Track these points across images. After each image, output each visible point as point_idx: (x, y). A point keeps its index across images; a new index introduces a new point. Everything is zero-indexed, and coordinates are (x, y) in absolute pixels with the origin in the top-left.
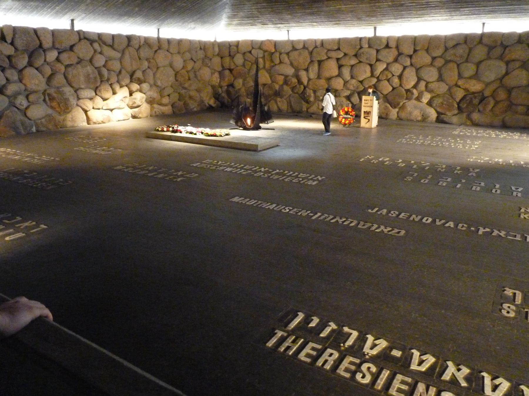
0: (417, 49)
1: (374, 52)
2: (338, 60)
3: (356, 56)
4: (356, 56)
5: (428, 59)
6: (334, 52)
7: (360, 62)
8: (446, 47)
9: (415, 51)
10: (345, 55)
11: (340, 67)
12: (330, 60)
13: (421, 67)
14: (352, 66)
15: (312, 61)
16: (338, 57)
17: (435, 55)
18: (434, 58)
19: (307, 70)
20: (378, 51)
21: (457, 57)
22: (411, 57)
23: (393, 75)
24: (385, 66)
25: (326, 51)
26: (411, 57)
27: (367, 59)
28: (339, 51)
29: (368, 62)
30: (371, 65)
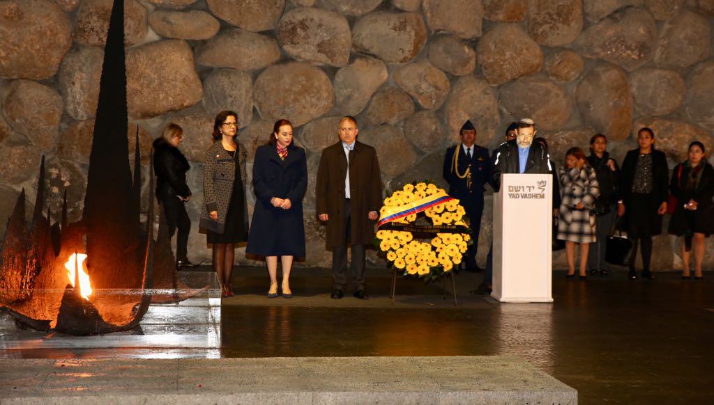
0: (501, 17)
1: (343, 25)
2: (197, 47)
3: (269, 34)
4: (269, 34)
5: (532, 54)
6: (181, 14)
7: (285, 59)
8: (585, 14)
9: (487, 26)
10: (226, 29)
11: (204, 74)
12: (167, 47)
13: (514, 80)
14: (256, 75)
15: (75, 48)
16: (198, 37)
17: (554, 40)
18: (548, 51)
19: (55, 82)
20: (352, 21)
21: (628, 48)
22: (474, 43)
23: (418, 108)
24: (385, 75)
25: (142, 12)
26: (474, 43)
27: (321, 47)
28: (204, 15)
29: (323, 59)
30: (332, 71)
